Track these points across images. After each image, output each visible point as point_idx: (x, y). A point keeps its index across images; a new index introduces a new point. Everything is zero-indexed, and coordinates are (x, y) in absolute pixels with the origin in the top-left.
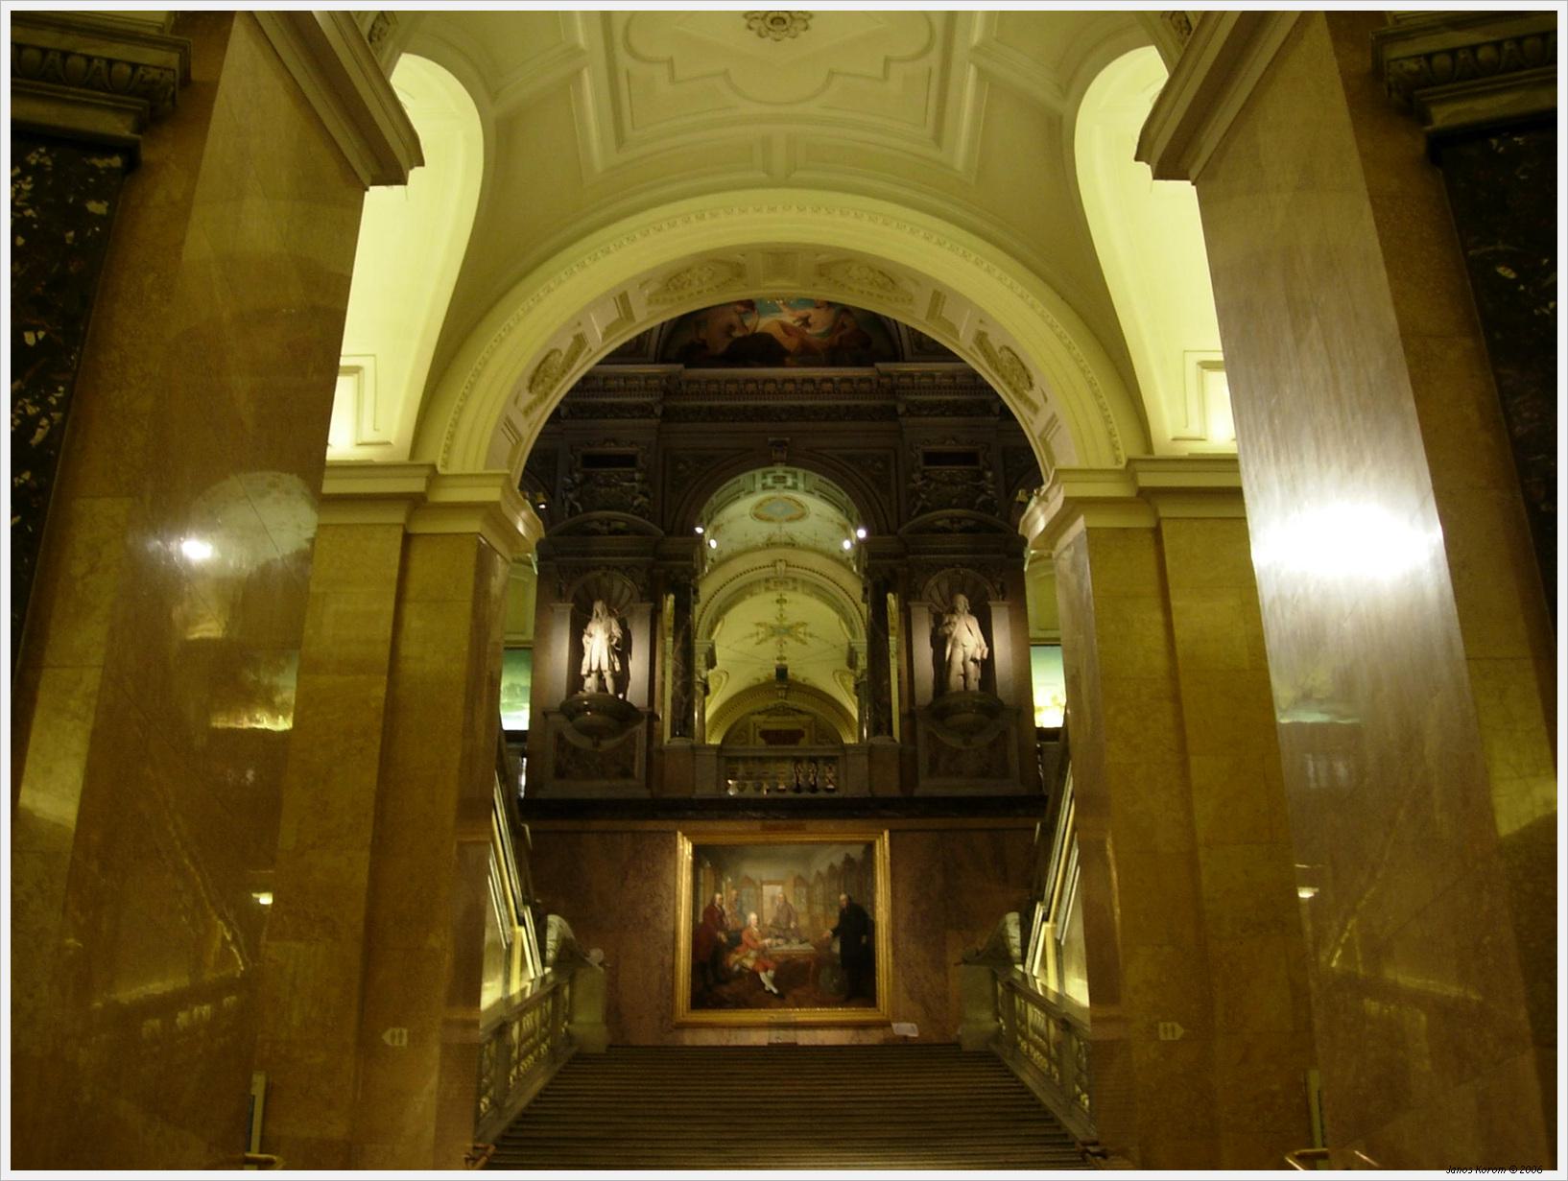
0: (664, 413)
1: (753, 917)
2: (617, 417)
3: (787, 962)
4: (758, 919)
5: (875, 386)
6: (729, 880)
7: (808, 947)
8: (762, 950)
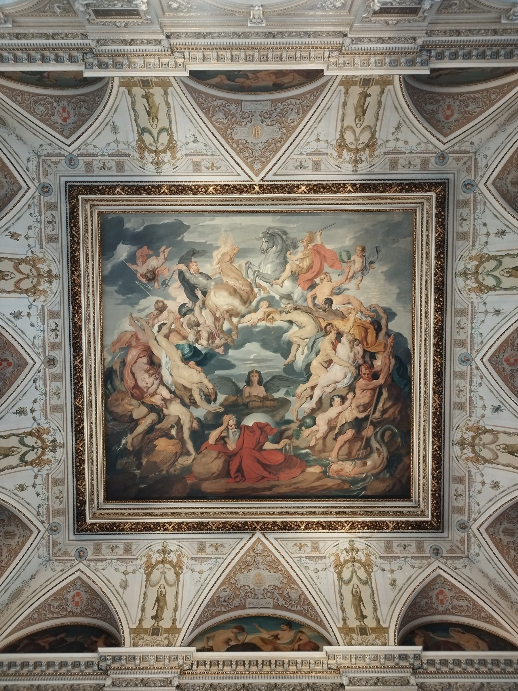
5: (325, 667)
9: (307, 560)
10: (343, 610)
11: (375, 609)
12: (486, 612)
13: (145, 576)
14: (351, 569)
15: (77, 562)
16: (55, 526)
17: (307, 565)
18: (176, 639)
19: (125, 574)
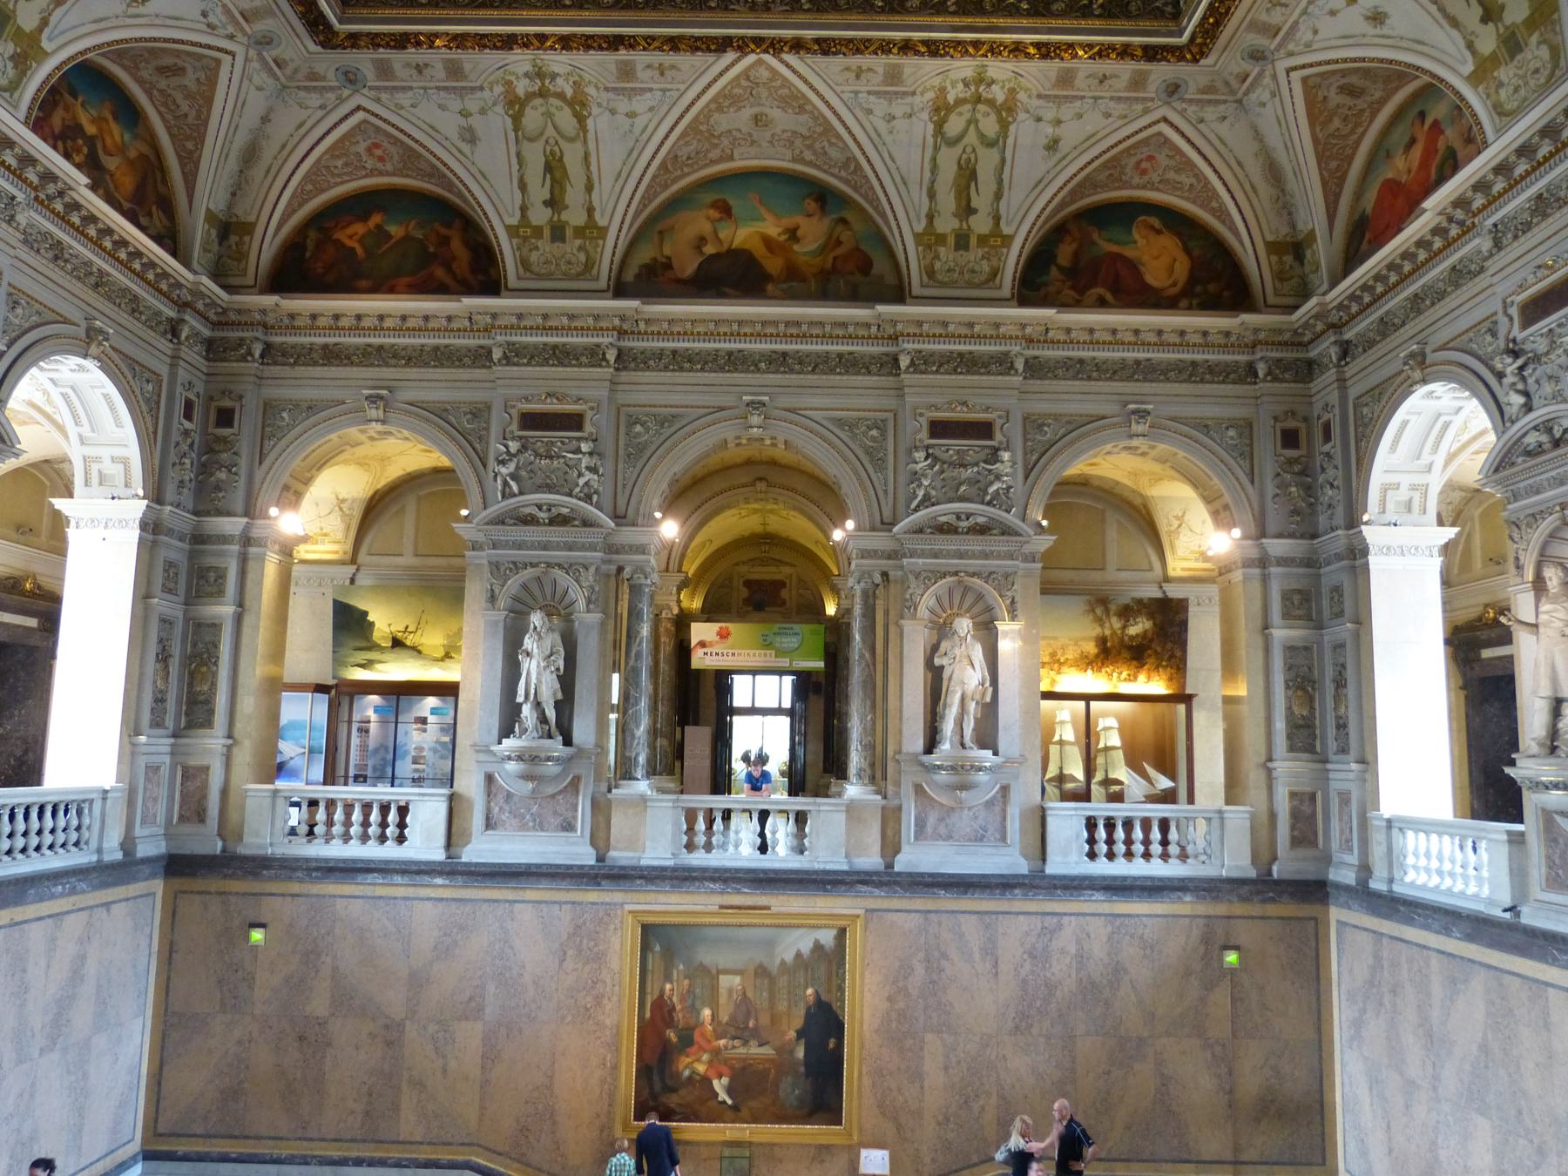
0: (619, 357)
1: (707, 1013)
2: (561, 364)
3: (744, 1069)
4: (713, 1015)
6: (681, 967)
7: (767, 1051)
8: (716, 1052)
9: (872, 98)
10: (932, 195)
11: (998, 196)
12: (1222, 205)
13: (509, 121)
14: (967, 116)
15: (346, 92)
16: (264, 37)
17: (871, 106)
18: (599, 250)
19: (466, 116)
